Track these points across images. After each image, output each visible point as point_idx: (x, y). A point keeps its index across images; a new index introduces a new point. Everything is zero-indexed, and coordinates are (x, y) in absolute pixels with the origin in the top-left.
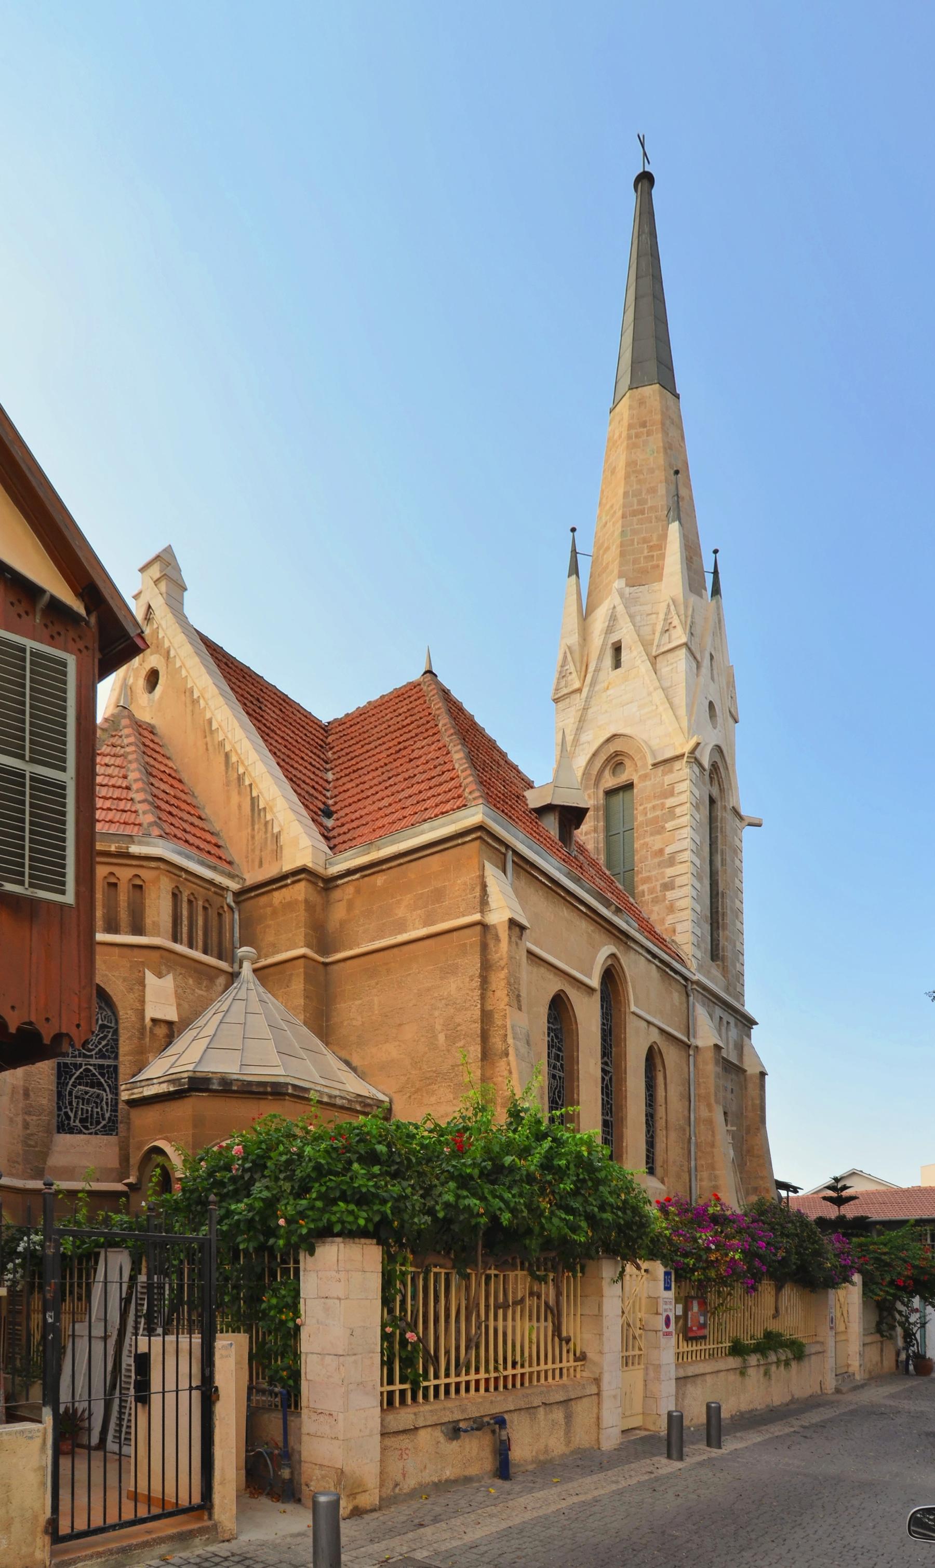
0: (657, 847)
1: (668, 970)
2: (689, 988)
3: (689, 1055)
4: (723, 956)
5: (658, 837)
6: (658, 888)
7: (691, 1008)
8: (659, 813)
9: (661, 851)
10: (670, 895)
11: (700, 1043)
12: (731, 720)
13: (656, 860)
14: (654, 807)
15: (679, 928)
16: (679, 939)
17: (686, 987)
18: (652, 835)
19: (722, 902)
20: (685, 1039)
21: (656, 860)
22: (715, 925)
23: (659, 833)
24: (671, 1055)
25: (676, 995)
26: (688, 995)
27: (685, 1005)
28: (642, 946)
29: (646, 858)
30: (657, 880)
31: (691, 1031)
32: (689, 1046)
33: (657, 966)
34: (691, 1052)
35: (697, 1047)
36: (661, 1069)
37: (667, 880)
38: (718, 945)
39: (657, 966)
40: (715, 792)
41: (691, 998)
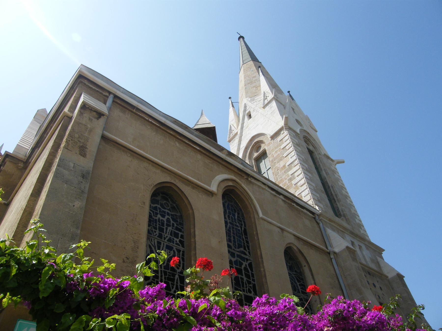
0: (282, 166)
1: (295, 205)
2: (317, 217)
3: (331, 259)
4: (344, 214)
5: (282, 162)
6: (288, 182)
7: (323, 232)
8: (279, 153)
9: (284, 166)
10: (294, 182)
11: (337, 250)
12: (315, 132)
13: (283, 171)
14: (276, 152)
15: (303, 194)
16: (305, 199)
17: (315, 218)
18: (278, 162)
19: (334, 191)
20: (324, 248)
21: (283, 171)
22: (333, 201)
23: (281, 160)
24: (312, 257)
25: (307, 222)
26: (318, 224)
27: (317, 229)
28: (264, 184)
29: (278, 173)
30: (286, 179)
31: (327, 243)
32: (329, 253)
33: (282, 200)
34: (332, 256)
35: (335, 253)
36: (306, 264)
37: (290, 176)
38: (338, 209)
39: (282, 200)
40: (311, 148)
41: (321, 224)
